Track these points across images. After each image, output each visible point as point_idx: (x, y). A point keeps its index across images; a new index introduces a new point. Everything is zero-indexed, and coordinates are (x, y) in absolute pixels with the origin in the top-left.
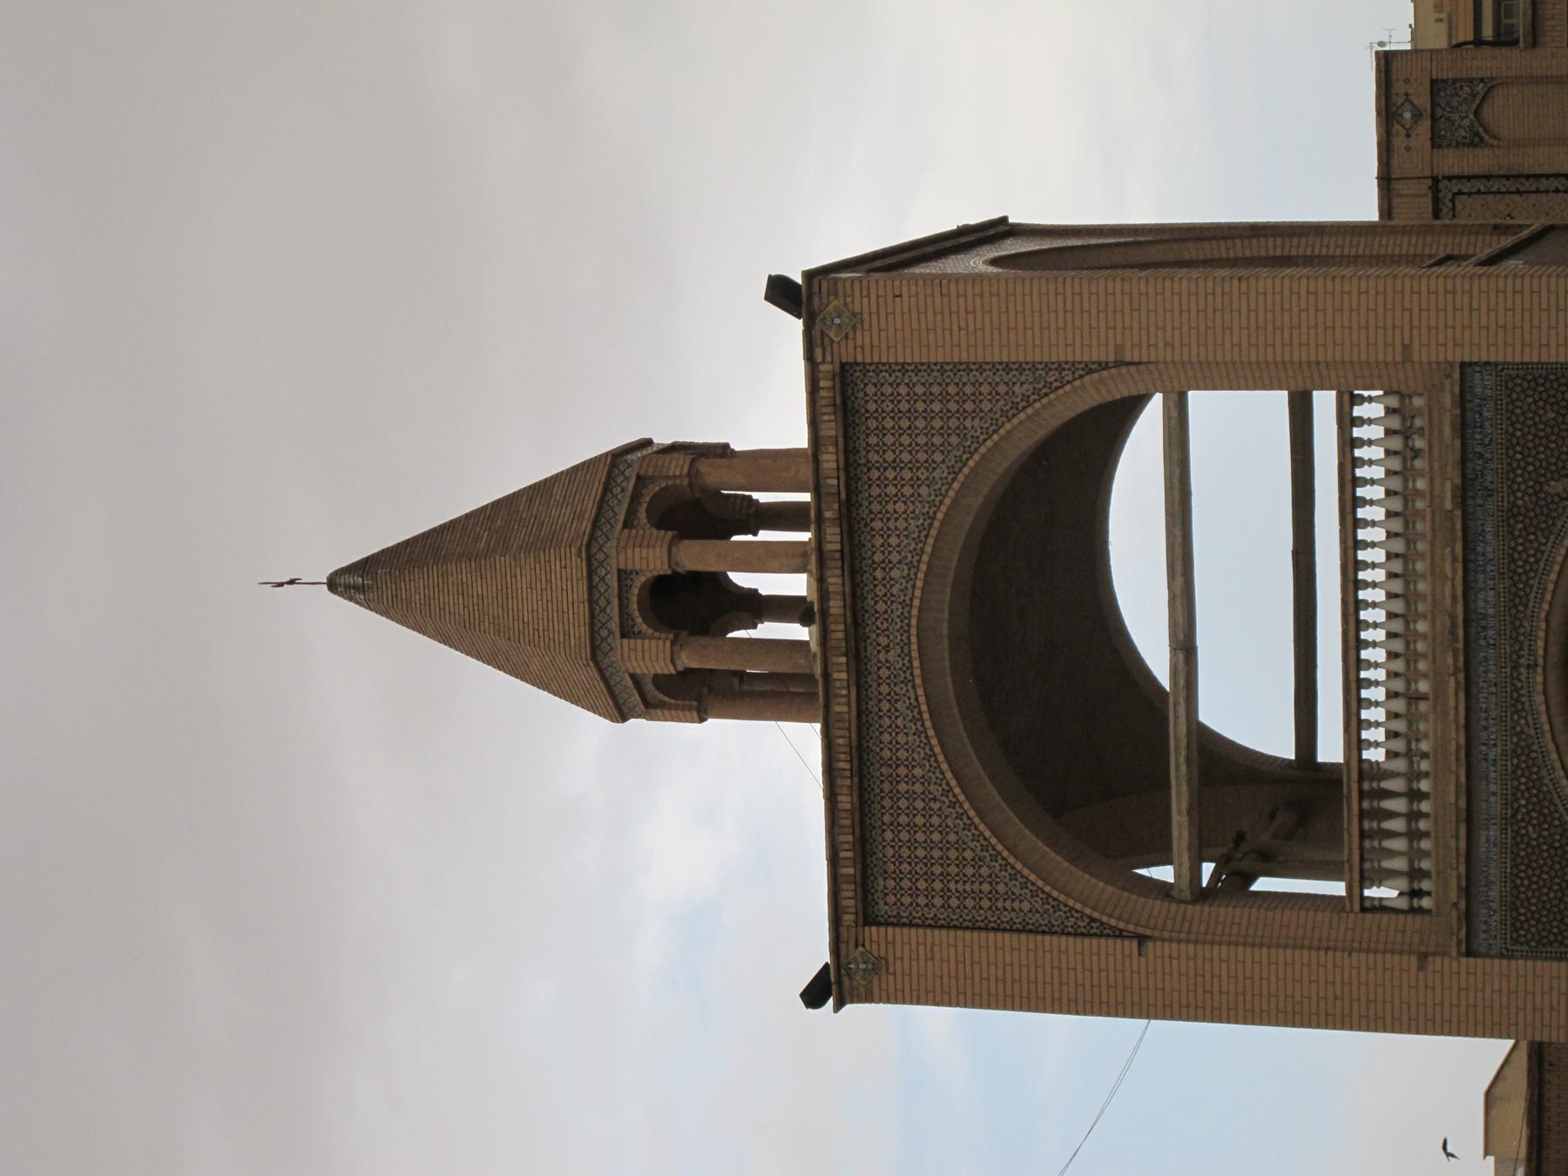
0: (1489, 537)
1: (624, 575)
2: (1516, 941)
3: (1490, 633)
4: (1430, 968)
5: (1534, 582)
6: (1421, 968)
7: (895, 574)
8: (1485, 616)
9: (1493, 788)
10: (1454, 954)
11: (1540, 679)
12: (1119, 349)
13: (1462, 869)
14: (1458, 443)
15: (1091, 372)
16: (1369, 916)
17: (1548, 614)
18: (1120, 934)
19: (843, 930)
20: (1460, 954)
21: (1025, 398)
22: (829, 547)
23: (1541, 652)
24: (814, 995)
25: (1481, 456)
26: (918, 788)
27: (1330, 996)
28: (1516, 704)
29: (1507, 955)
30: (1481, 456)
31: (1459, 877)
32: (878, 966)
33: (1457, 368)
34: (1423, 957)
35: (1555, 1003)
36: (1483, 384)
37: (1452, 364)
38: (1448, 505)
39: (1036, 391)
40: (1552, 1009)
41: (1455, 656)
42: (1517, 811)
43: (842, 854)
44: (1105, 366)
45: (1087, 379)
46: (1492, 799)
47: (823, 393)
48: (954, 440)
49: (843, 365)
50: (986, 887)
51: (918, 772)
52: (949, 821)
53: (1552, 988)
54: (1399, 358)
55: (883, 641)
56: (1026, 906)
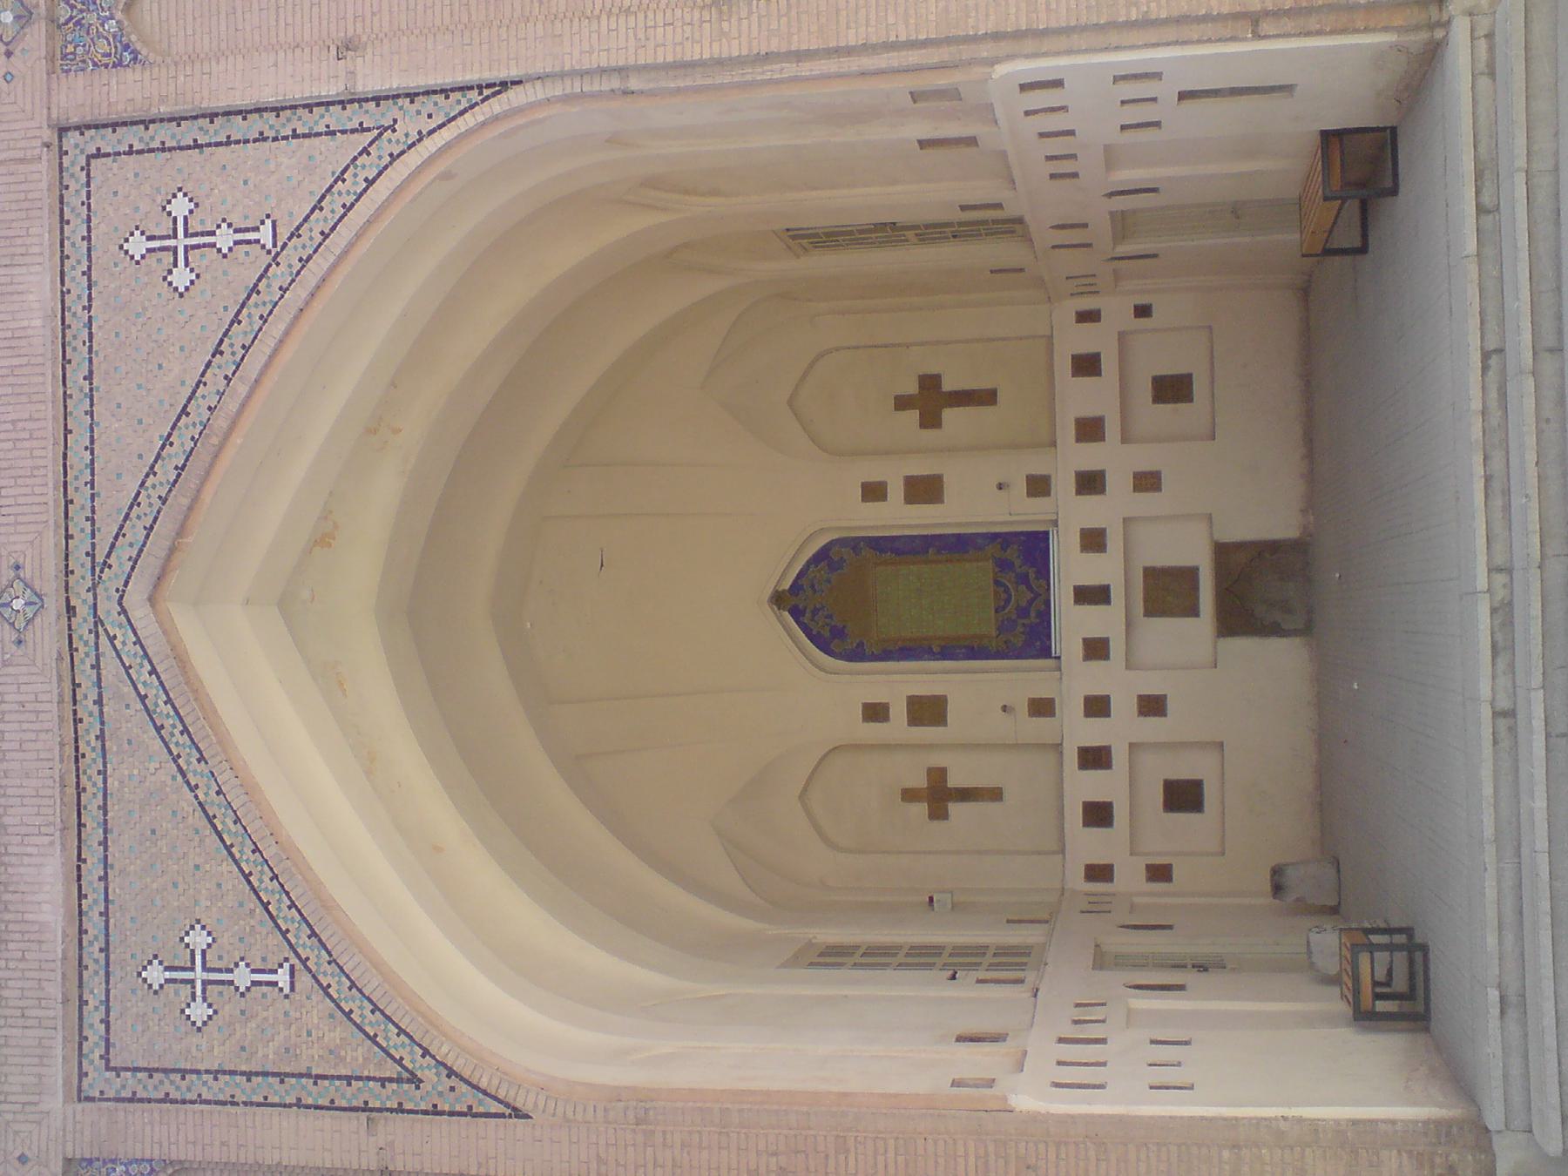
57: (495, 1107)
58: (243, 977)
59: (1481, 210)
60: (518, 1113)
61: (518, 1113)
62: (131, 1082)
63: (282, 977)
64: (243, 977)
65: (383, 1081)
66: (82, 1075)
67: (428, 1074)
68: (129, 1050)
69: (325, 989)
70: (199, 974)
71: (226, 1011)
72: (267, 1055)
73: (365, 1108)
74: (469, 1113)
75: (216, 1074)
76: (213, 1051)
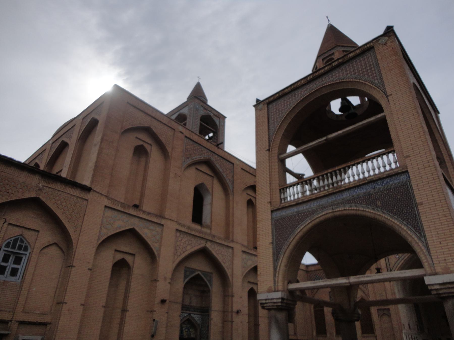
0: (362, 191)
1: (333, 54)
2: (275, 220)
3: (339, 198)
5: (353, 204)
8: (343, 195)
11: (330, 211)
13: (287, 205)
14: (385, 176)
15: (384, 93)
16: (279, 191)
17: (346, 210)
18: (269, 146)
23: (336, 210)
25: (383, 183)
28: (323, 208)
29: (272, 219)
32: (261, 110)
33: (405, 170)
34: (270, 203)
36: (403, 178)
37: (407, 168)
38: (368, 179)
45: (382, 92)
47: (366, 46)
51: (294, 100)
54: (405, 155)
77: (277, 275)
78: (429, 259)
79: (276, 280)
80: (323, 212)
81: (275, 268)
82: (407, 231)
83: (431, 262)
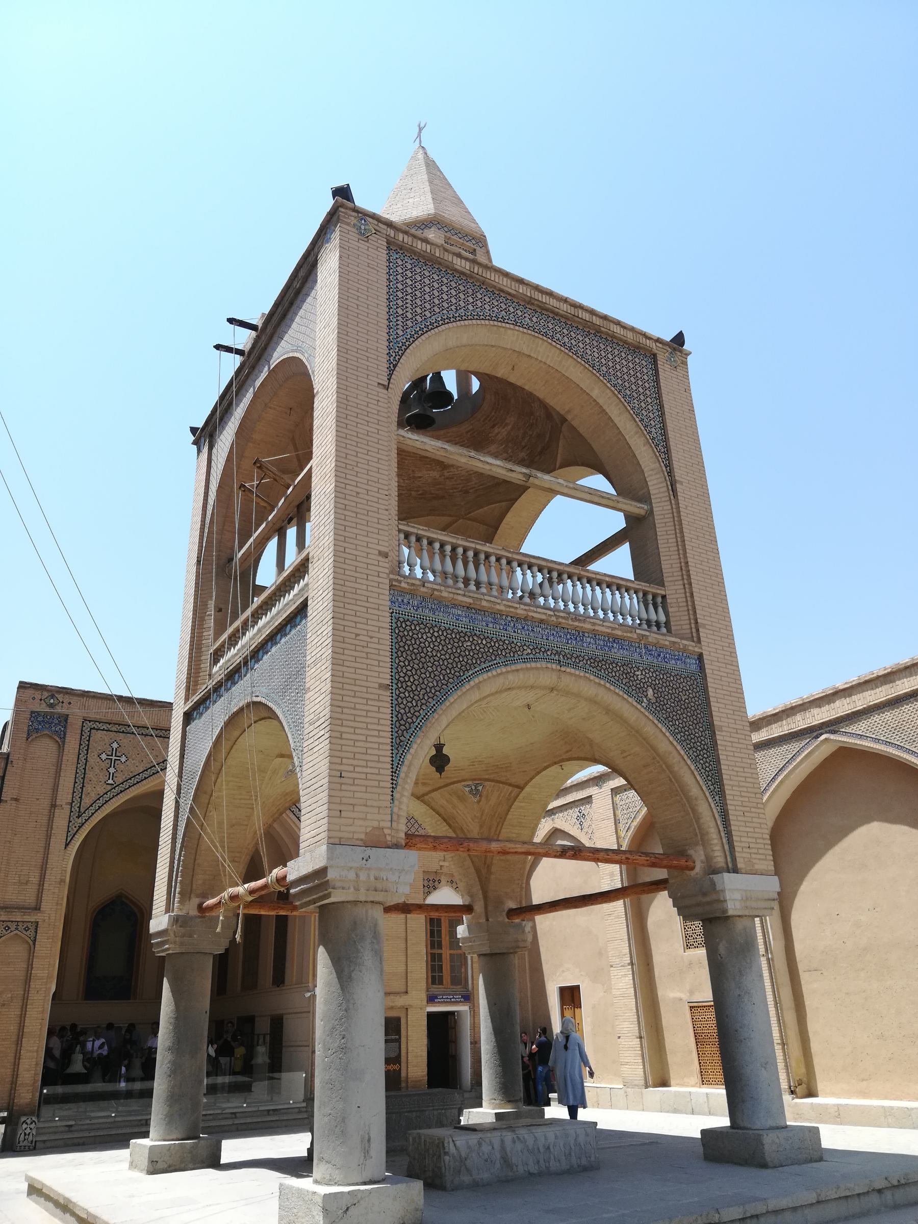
4: (380, 558)
6: (381, 553)
7: (566, 339)
9: (491, 625)
10: (391, 576)
12: (681, 483)
18: (390, 376)
19: (385, 227)
20: (391, 580)
21: (650, 432)
22: (580, 311)
24: (343, 193)
26: (462, 304)
27: (358, 490)
30: (659, 655)
31: (441, 591)
35: (361, 637)
39: (654, 438)
40: (357, 635)
41: (563, 618)
42: (478, 637)
43: (428, 246)
44: (670, 473)
46: (484, 624)
48: (629, 393)
49: (655, 355)
50: (410, 316)
52: (445, 312)
53: (371, 637)
55: (534, 319)
56: (401, 333)
57: (69, 839)
58: (112, 770)
59: (269, 1111)
60: (67, 845)
61: (67, 845)
62: (86, 735)
63: (110, 781)
64: (112, 770)
65: (79, 807)
66: (90, 721)
67: (80, 820)
68: (97, 736)
69: (106, 793)
70: (114, 758)
71: (103, 764)
72: (89, 775)
73: (73, 802)
74: (68, 831)
75: (86, 759)
76: (93, 759)
77: (396, 795)
78: (725, 840)
79: (396, 810)
80: (536, 660)
81: (395, 772)
82: (696, 773)
83: (726, 847)
